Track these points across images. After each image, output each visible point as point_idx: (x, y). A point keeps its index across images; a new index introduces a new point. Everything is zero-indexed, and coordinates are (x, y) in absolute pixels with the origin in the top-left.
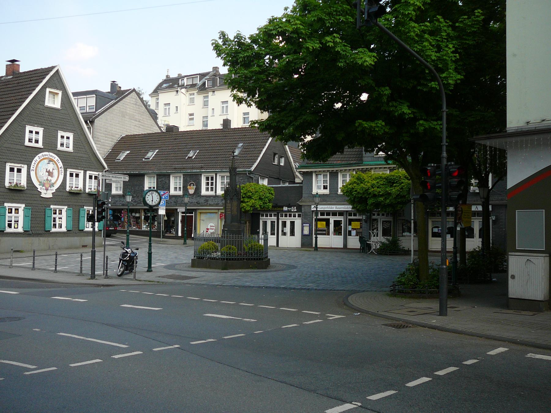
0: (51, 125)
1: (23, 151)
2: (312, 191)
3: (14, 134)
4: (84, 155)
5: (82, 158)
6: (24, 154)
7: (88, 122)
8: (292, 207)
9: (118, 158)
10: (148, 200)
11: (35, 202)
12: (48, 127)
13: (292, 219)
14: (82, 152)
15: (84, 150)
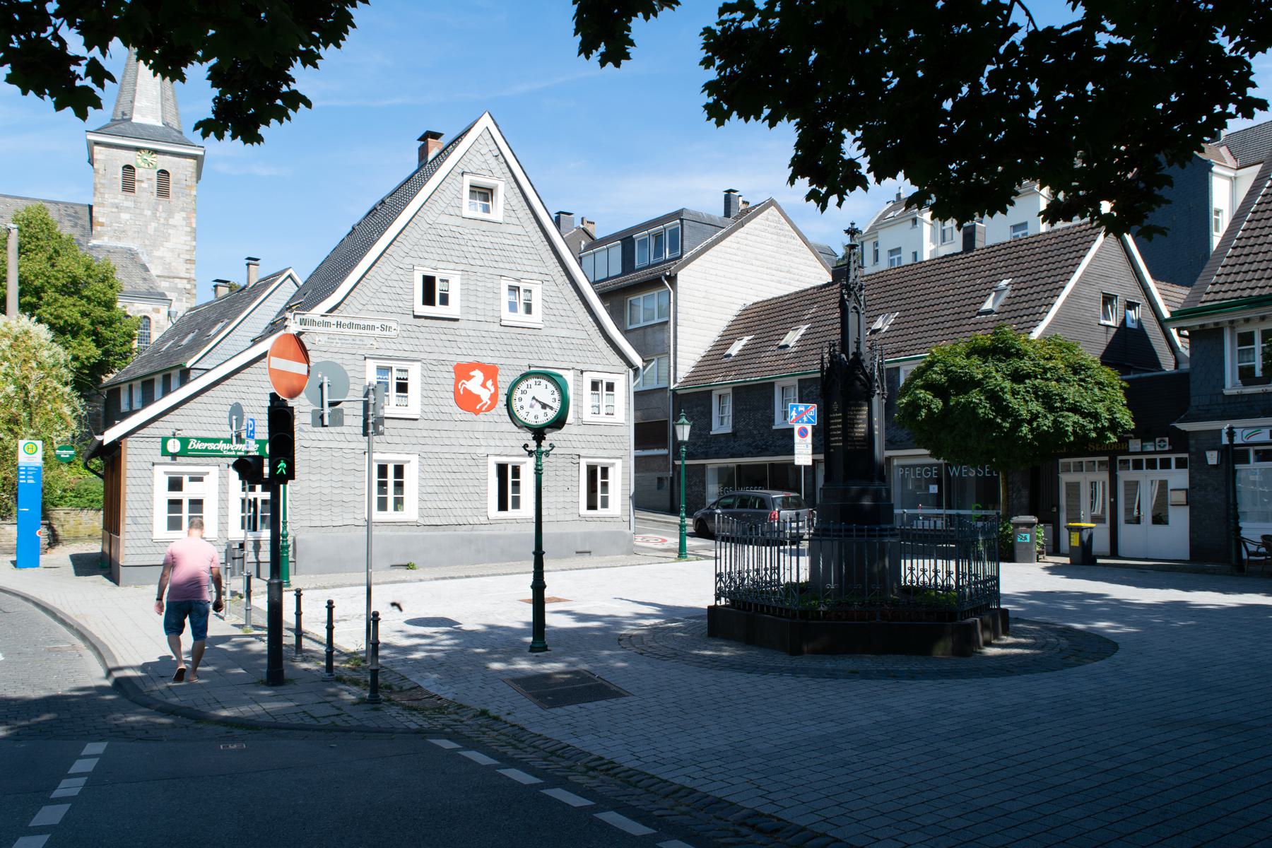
0: (480, 263)
1: (409, 328)
2: (1224, 386)
3: (384, 289)
4: (573, 334)
5: (568, 341)
6: (413, 335)
7: (663, 278)
8: (1157, 440)
9: (728, 352)
10: (522, 407)
11: (445, 449)
12: (474, 269)
13: (1159, 474)
14: (570, 326)
15: (573, 320)
